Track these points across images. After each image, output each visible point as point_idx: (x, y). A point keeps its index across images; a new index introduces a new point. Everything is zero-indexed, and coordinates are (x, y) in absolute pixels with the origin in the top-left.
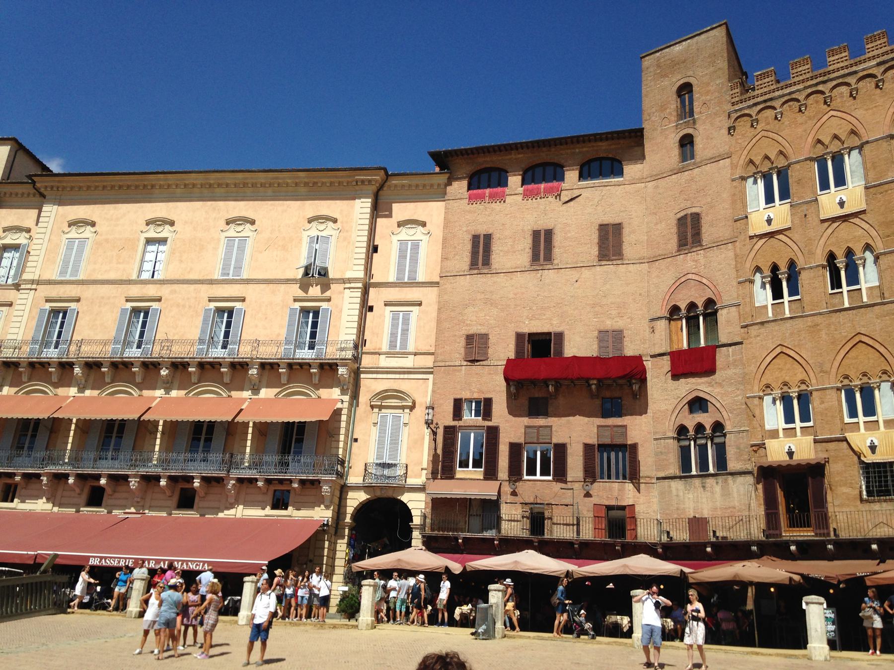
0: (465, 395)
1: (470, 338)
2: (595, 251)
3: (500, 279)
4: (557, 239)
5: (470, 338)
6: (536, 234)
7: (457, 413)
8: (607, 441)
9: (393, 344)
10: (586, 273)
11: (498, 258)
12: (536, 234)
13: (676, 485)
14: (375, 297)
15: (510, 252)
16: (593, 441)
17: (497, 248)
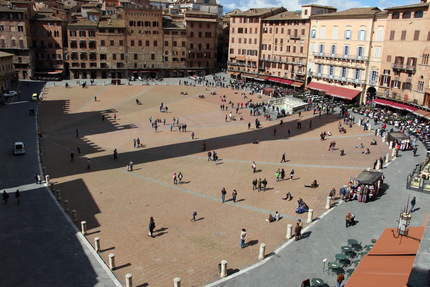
0: (386, 69)
1: (388, 56)
2: (413, 38)
3: (395, 43)
4: (407, 34)
5: (388, 56)
6: (403, 32)
7: (384, 73)
8: (408, 82)
9: (375, 56)
10: (411, 43)
11: (395, 37)
12: (403, 32)
13: (416, 92)
14: (373, 44)
15: (398, 36)
16: (405, 82)
17: (395, 35)
